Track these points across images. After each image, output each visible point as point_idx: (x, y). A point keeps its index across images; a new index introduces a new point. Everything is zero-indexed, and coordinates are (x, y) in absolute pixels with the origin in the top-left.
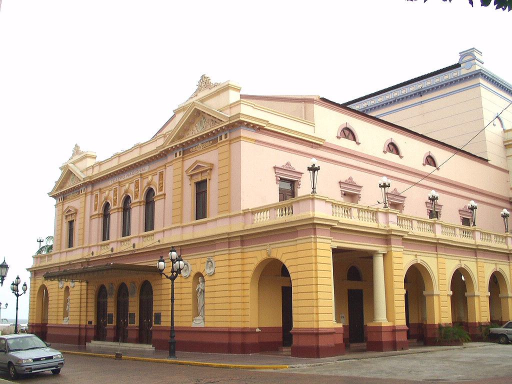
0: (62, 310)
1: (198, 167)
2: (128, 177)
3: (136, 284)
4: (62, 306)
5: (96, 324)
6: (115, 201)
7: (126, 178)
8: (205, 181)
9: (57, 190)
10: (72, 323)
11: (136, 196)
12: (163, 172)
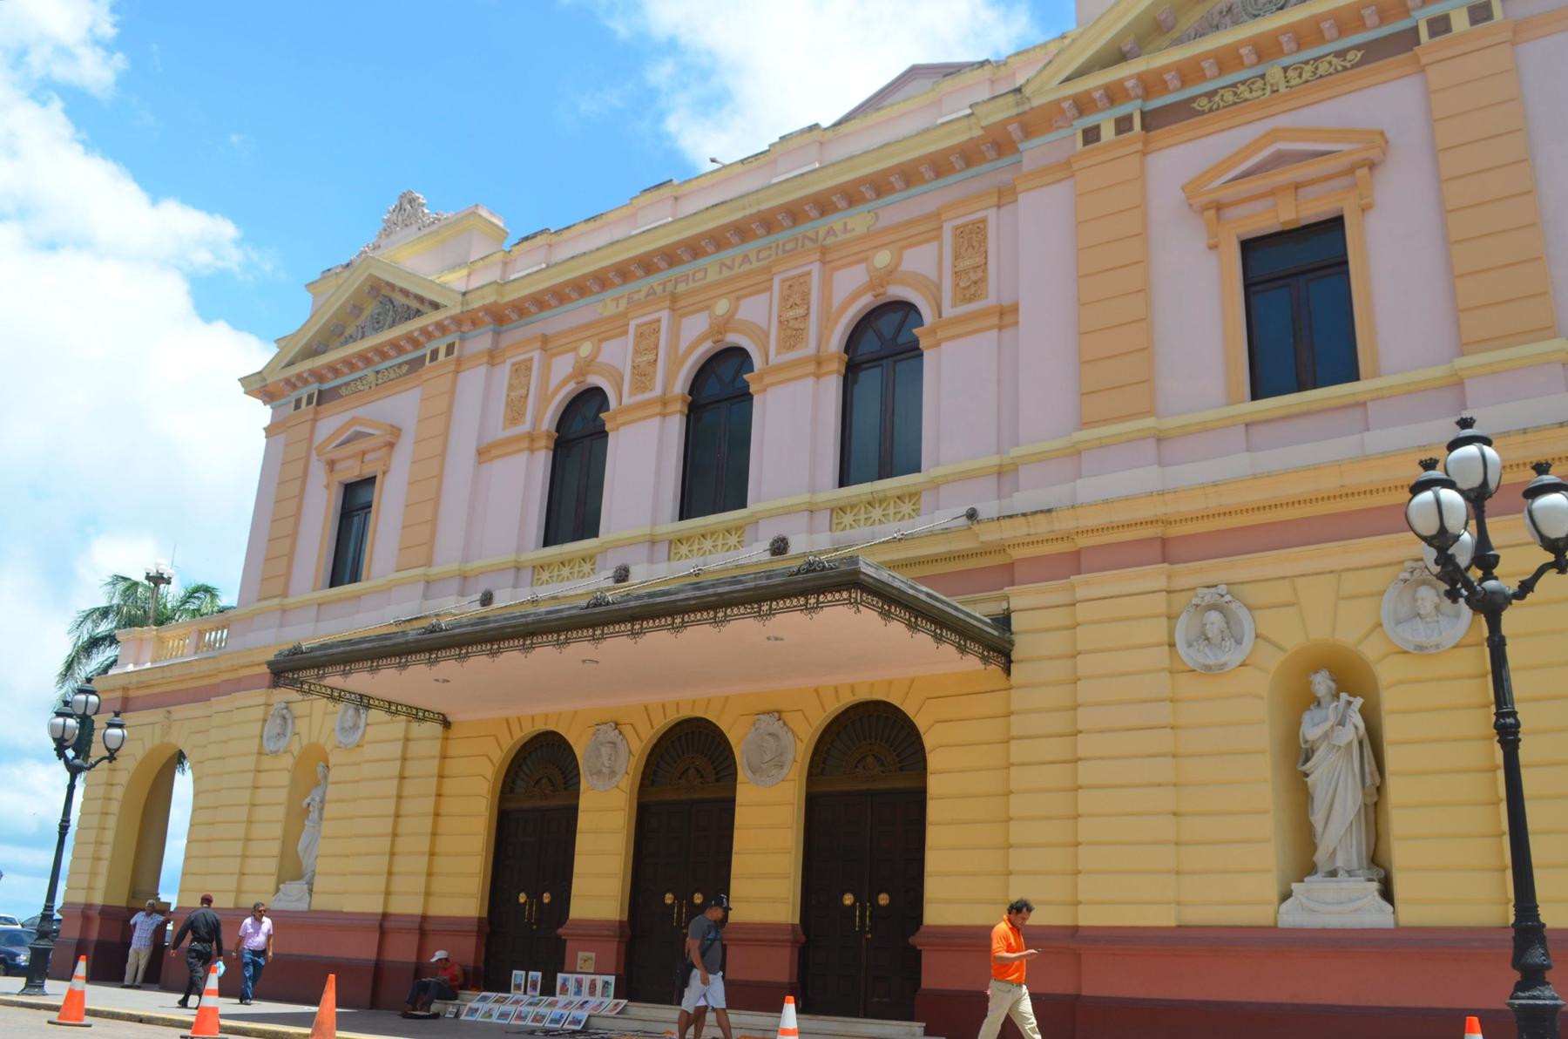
0: (275, 848)
1: (1280, 160)
2: (726, 273)
3: (795, 721)
4: (277, 830)
5: (485, 914)
6: (642, 377)
7: (713, 276)
8: (1335, 224)
9: (291, 363)
10: (322, 902)
11: (792, 335)
12: (984, 220)
